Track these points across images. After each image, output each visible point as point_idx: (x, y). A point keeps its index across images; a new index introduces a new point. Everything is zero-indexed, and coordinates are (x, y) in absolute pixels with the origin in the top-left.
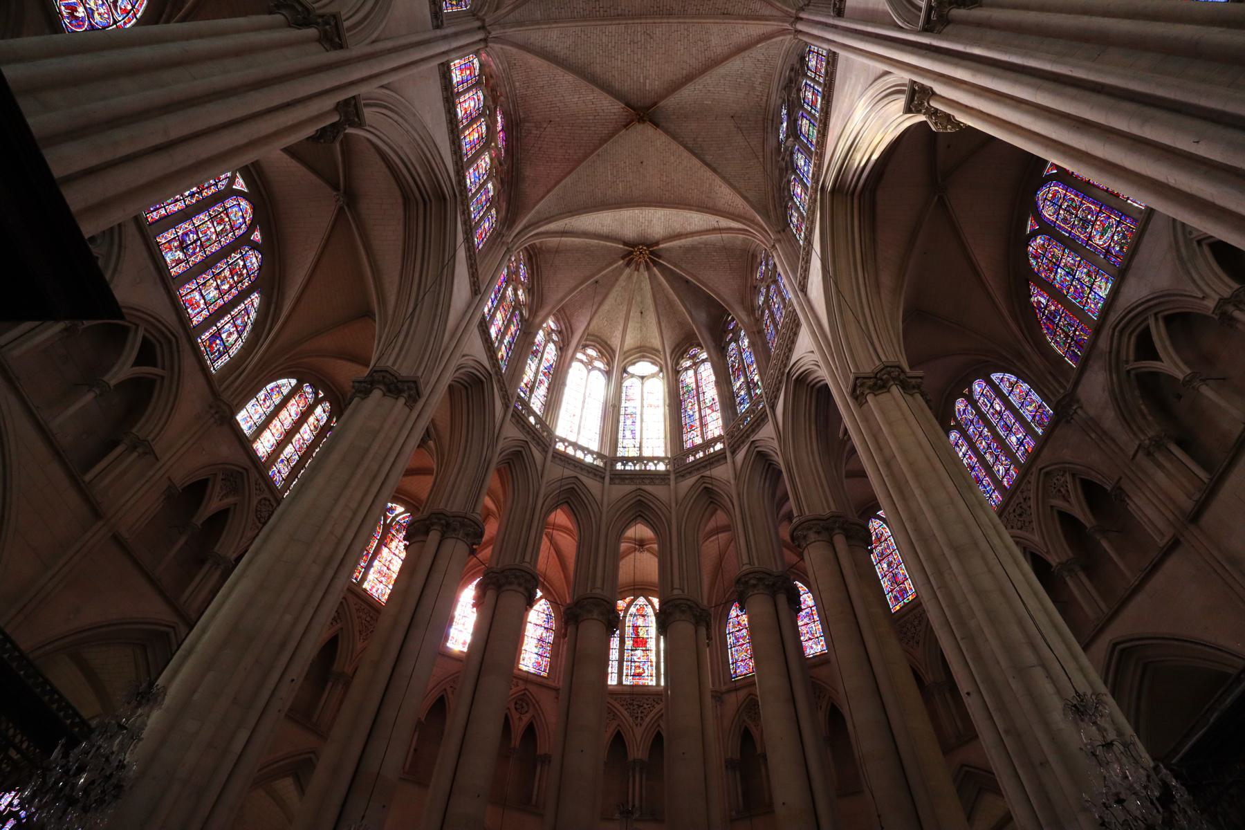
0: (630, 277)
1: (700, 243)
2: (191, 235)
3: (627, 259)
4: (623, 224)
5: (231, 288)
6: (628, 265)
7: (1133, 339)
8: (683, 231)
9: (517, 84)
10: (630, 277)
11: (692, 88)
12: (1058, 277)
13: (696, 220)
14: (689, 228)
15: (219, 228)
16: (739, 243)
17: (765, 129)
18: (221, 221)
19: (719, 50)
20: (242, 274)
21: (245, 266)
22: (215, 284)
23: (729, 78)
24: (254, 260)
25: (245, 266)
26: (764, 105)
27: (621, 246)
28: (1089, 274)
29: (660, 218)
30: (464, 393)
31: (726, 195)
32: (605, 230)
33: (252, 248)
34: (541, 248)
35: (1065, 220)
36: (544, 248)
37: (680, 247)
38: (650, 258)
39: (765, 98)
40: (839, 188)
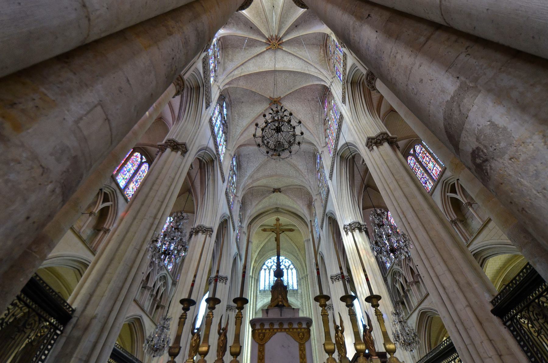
0: (280, 30)
1: (248, 49)
2: (423, 180)
3: (281, 42)
4: (283, 58)
5: (427, 156)
6: (281, 39)
7: (108, 193)
8: (256, 58)
9: (317, 116)
10: (280, 30)
11: (258, 111)
12: (130, 164)
13: (252, 68)
14: (254, 60)
15: (417, 169)
16: (230, 52)
17: (230, 101)
18: (415, 169)
19: (251, 126)
20: (423, 153)
21: (420, 153)
22: (429, 165)
23: (246, 116)
24: (417, 149)
25: (420, 153)
26: (232, 108)
27: (284, 49)
28: (126, 179)
29: (267, 62)
30: (361, 82)
31: (242, 84)
32: (291, 57)
33: (416, 152)
34: (321, 47)
35: (139, 174)
36: (320, 48)
37: (256, 47)
38: (270, 42)
39: (233, 111)
40: (212, 161)
